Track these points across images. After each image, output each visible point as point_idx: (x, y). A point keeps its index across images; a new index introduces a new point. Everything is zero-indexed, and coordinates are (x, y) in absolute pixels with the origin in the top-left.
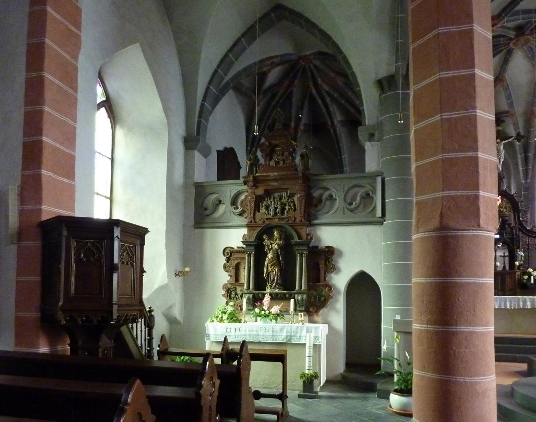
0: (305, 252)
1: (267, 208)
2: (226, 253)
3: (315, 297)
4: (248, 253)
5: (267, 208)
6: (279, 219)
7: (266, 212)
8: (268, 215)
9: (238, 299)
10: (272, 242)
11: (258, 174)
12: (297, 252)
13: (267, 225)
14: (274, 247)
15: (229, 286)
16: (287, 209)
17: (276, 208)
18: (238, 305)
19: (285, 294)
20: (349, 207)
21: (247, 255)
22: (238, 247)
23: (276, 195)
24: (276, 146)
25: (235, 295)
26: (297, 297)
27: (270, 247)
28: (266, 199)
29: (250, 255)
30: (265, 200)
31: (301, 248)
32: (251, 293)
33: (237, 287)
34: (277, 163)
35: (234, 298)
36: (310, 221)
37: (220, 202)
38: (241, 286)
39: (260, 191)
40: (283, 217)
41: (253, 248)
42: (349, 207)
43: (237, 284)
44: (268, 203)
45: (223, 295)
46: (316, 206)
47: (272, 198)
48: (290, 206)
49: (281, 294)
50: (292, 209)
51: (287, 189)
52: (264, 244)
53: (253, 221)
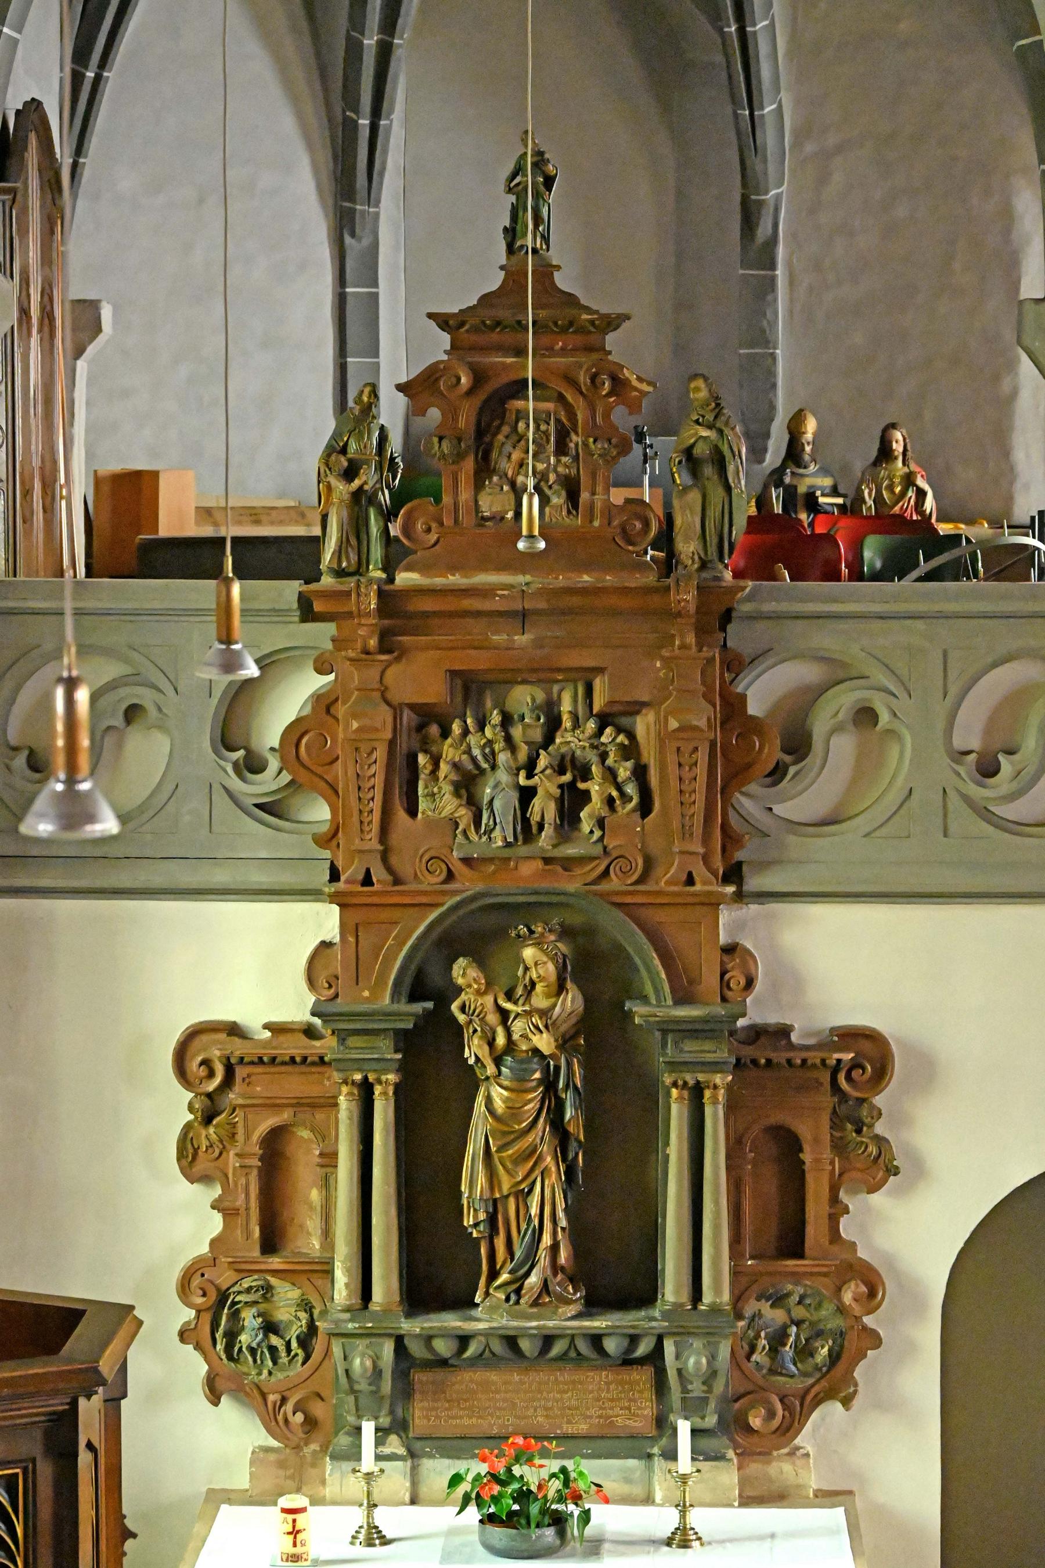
0: (718, 1079)
2: (193, 1066)
3: (778, 1339)
4: (358, 1077)
6: (547, 861)
7: (464, 815)
8: (473, 836)
9: (284, 1359)
10: (508, 1006)
11: (405, 578)
12: (668, 1080)
13: (473, 898)
14: (525, 1036)
15: (225, 1278)
16: (595, 797)
17: (527, 795)
18: (284, 1400)
19: (596, 1340)
20: (974, 790)
21: (345, 1089)
22: (277, 1029)
25: (266, 1336)
26: (678, 1357)
27: (501, 1040)
28: (456, 728)
29: (366, 1091)
30: (446, 733)
31: (692, 1050)
32: (389, 1335)
33: (273, 1281)
35: (253, 1351)
36: (733, 874)
37: (132, 713)
38: (303, 1278)
40: (571, 850)
41: (387, 1050)
42: (974, 790)
43: (275, 1262)
44: (468, 751)
45: (184, 1335)
46: (777, 773)
47: (496, 718)
48: (611, 774)
49: (573, 1336)
50: (625, 798)
51: (600, 670)
52: (462, 1018)
53: (379, 874)
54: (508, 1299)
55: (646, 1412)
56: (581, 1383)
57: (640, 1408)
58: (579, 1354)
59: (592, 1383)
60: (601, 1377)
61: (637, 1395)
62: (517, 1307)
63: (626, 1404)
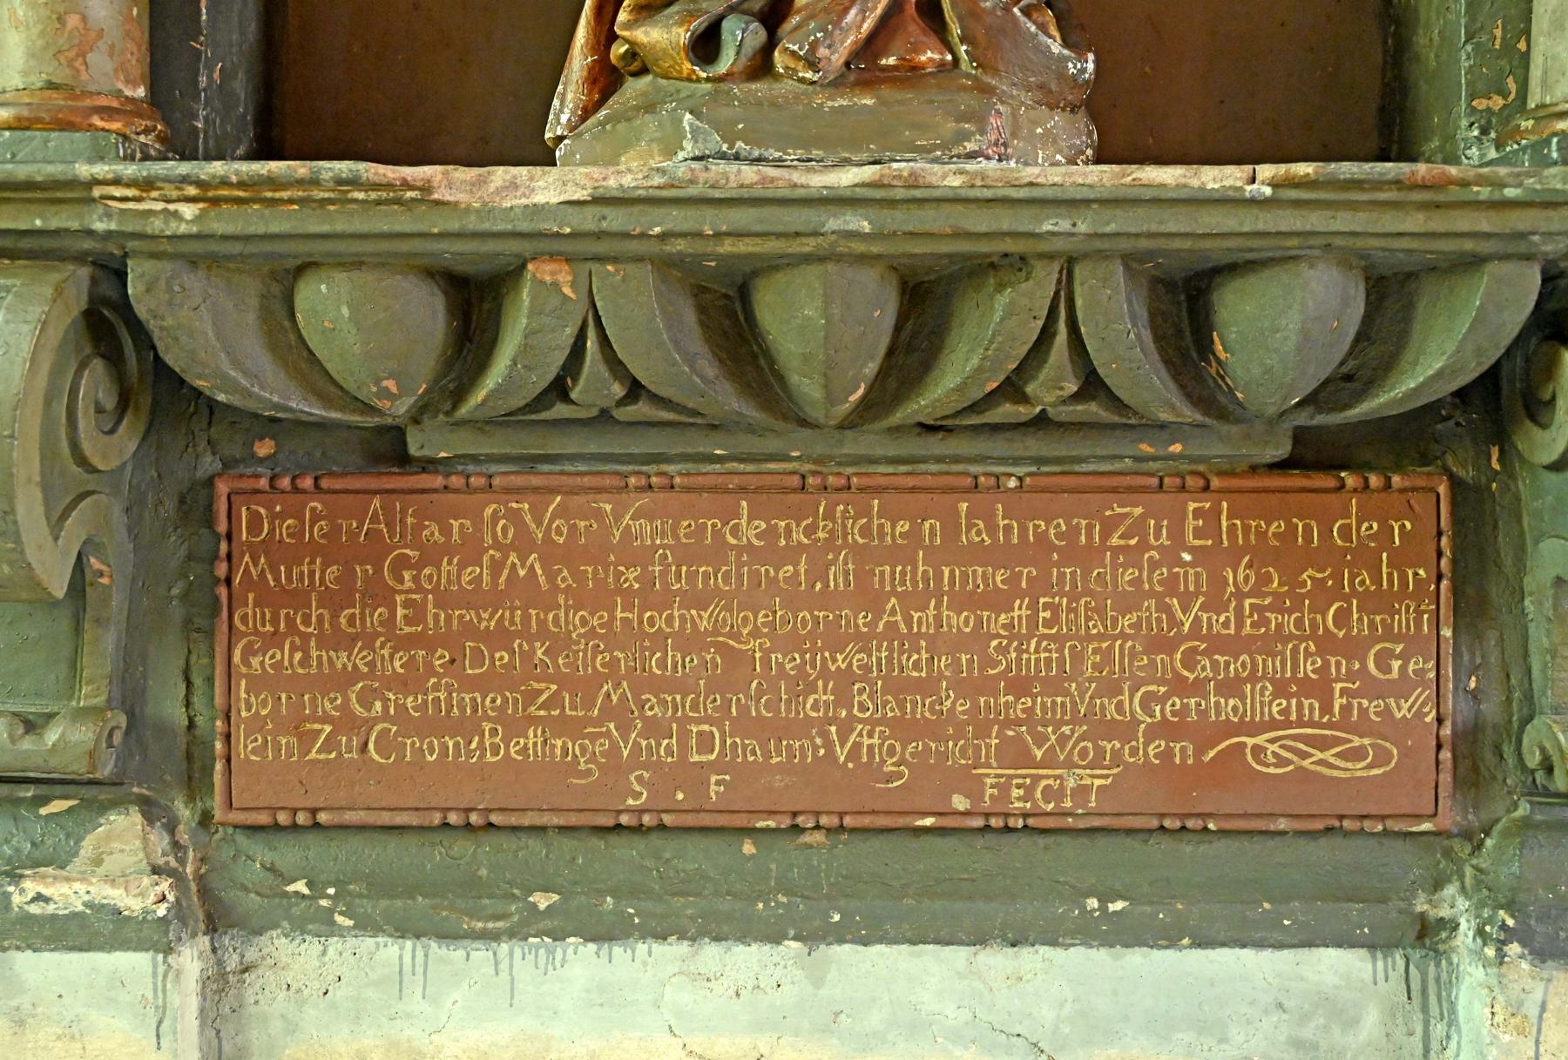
49: (1070, 262)
54: (706, 45)
55: (1402, 711)
56: (1072, 553)
57: (1375, 690)
58: (1092, 385)
59: (1132, 556)
60: (1177, 534)
61: (1359, 623)
62: (759, 88)
63: (1308, 668)
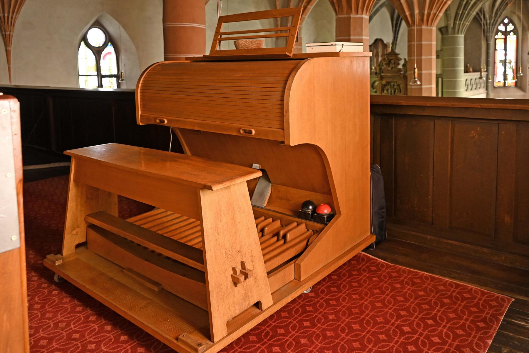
1: (387, 90)
5: (387, 90)
17: (391, 91)
23: (392, 84)
24: (392, 59)
34: (392, 68)
39: (384, 82)
48: (398, 90)
